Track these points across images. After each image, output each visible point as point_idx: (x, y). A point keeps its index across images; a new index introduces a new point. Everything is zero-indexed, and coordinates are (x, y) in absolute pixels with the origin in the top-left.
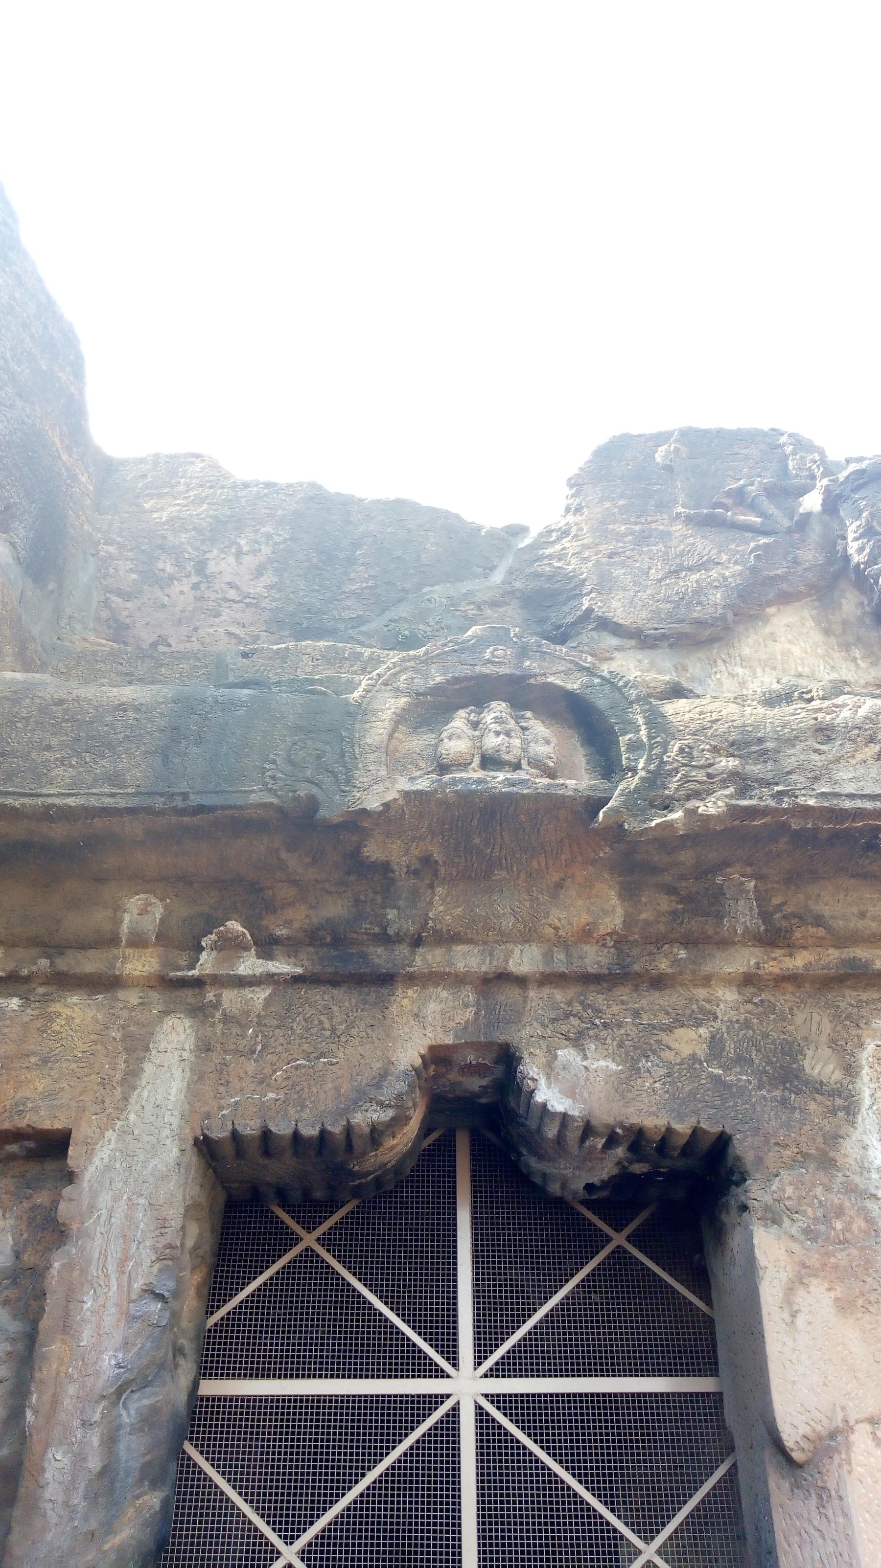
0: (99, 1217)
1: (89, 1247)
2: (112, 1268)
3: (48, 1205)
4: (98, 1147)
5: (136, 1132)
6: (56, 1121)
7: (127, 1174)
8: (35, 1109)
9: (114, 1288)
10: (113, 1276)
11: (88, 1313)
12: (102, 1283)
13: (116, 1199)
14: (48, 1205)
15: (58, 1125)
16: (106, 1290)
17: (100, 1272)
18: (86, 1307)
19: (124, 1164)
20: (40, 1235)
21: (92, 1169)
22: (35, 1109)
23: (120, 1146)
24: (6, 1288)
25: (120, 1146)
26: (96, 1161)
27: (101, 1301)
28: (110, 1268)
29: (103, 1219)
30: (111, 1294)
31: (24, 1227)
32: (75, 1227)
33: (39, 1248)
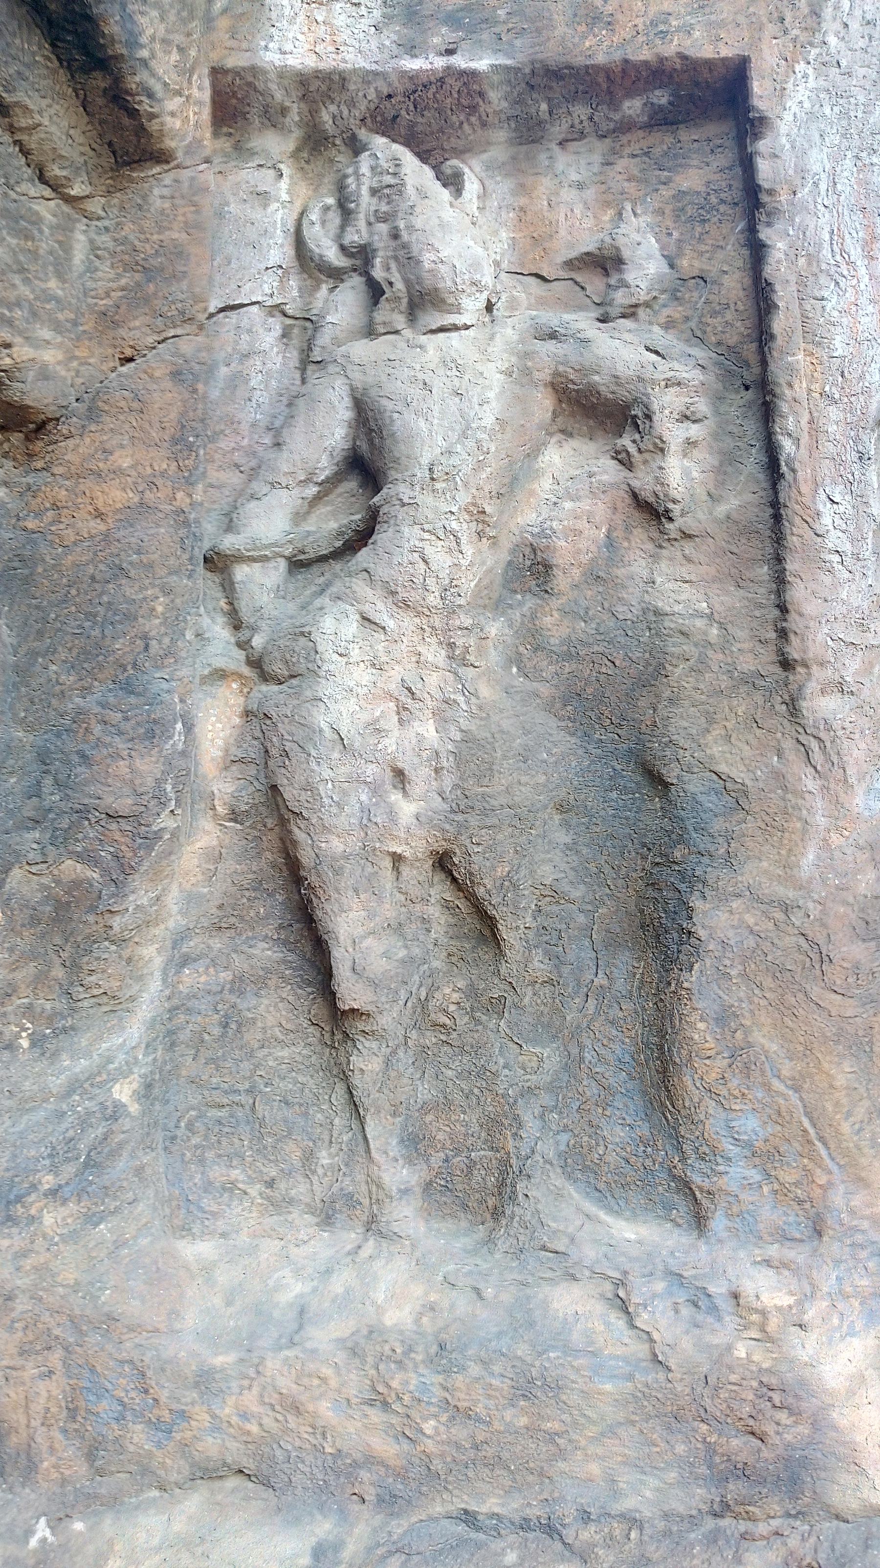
0: (816, 184)
1: (812, 226)
2: (855, 252)
3: (702, 189)
4: (789, 86)
5: (844, 63)
6: (721, 44)
7: (844, 123)
8: (685, 29)
9: (866, 279)
10: (859, 263)
11: (835, 314)
12: (845, 273)
13: (837, 159)
14: (702, 189)
15: (726, 52)
16: (854, 282)
17: (838, 258)
18: (829, 306)
19: (836, 109)
20: (699, 229)
21: (788, 117)
22: (685, 29)
23: (822, 83)
24: (664, 306)
25: (822, 83)
26: (791, 104)
27: (850, 295)
28: (852, 252)
29: (823, 186)
30: (862, 287)
31: (669, 223)
32: (784, 197)
33: (703, 248)
